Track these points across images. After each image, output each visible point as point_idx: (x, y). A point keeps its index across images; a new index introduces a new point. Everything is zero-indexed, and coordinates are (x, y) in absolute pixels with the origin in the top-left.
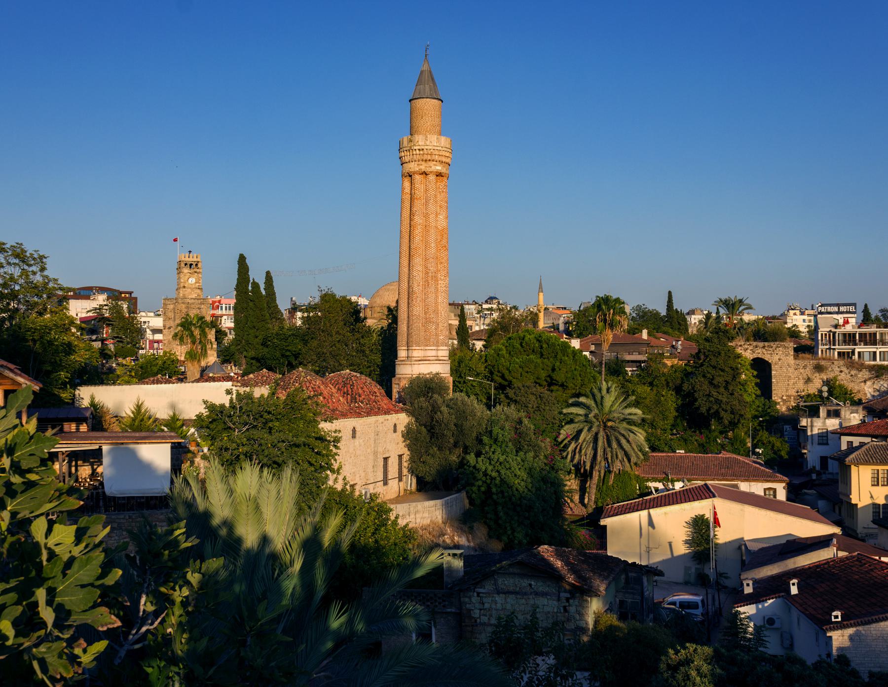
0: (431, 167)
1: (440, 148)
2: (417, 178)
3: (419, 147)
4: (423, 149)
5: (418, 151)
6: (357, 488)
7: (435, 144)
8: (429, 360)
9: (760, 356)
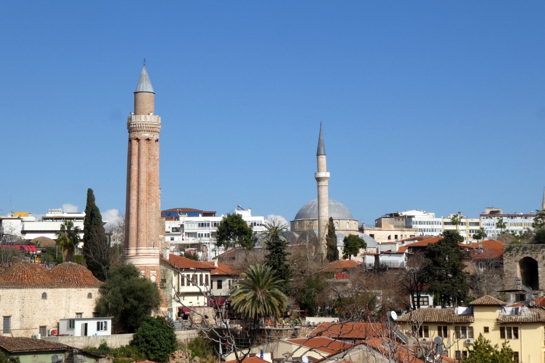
0: (141, 135)
1: (147, 123)
2: (134, 142)
3: (133, 123)
4: (136, 124)
5: (133, 125)
6: (47, 328)
7: (144, 121)
8: (151, 256)
9: (529, 255)
